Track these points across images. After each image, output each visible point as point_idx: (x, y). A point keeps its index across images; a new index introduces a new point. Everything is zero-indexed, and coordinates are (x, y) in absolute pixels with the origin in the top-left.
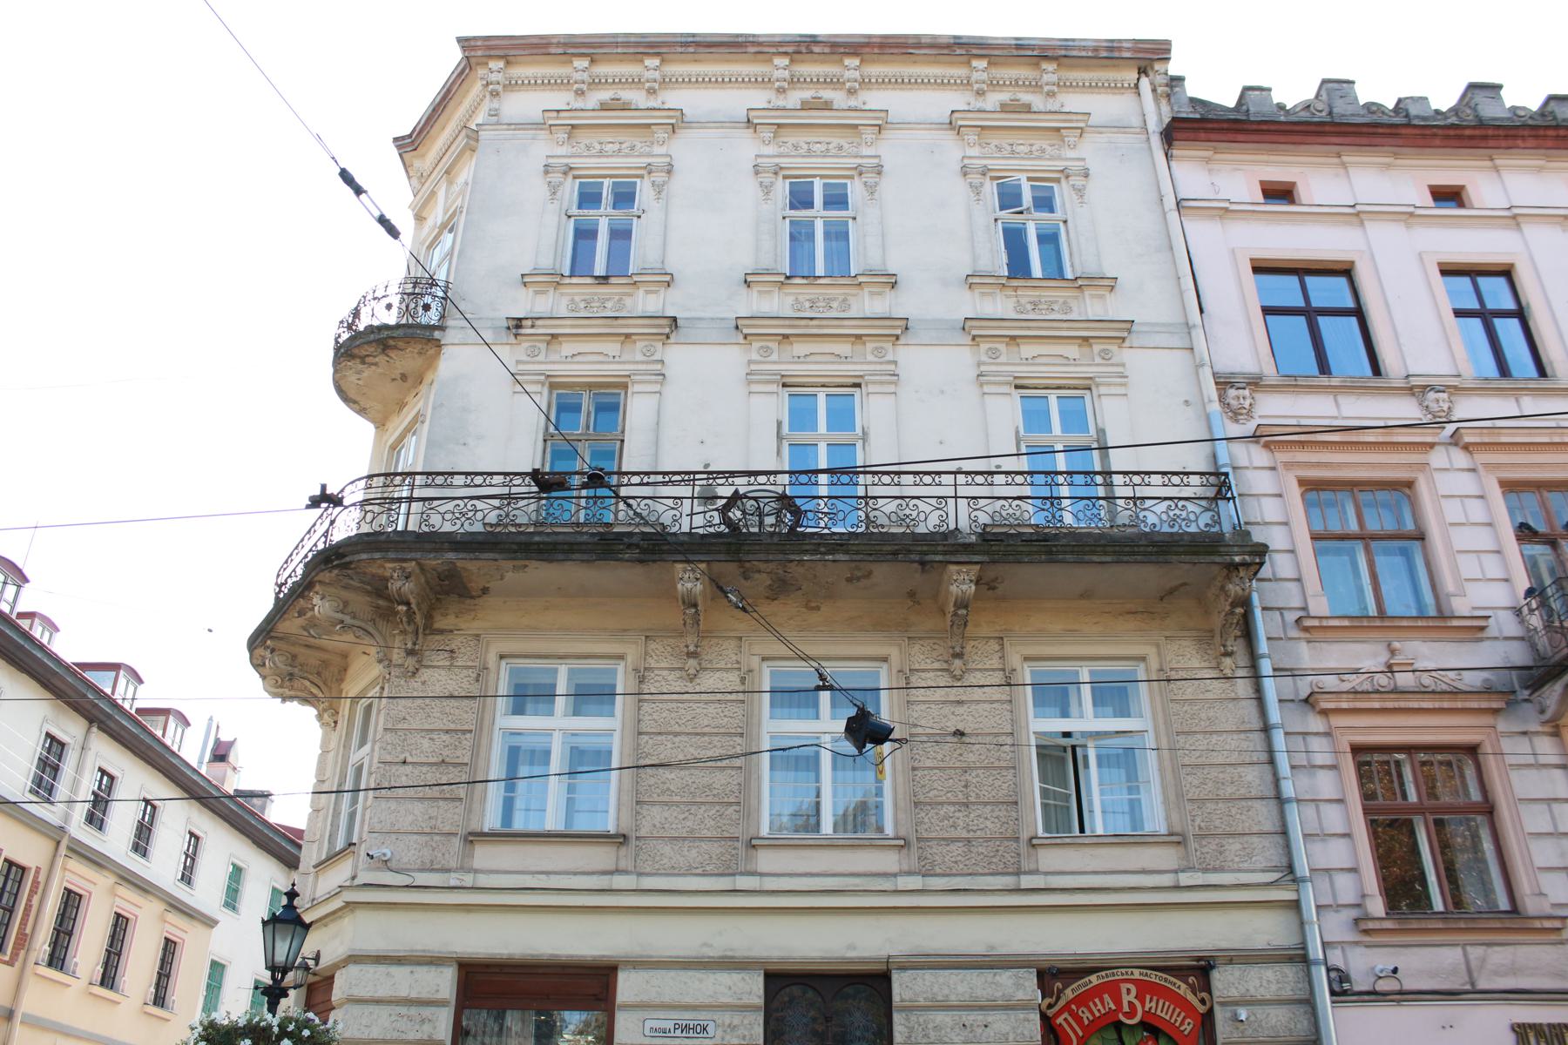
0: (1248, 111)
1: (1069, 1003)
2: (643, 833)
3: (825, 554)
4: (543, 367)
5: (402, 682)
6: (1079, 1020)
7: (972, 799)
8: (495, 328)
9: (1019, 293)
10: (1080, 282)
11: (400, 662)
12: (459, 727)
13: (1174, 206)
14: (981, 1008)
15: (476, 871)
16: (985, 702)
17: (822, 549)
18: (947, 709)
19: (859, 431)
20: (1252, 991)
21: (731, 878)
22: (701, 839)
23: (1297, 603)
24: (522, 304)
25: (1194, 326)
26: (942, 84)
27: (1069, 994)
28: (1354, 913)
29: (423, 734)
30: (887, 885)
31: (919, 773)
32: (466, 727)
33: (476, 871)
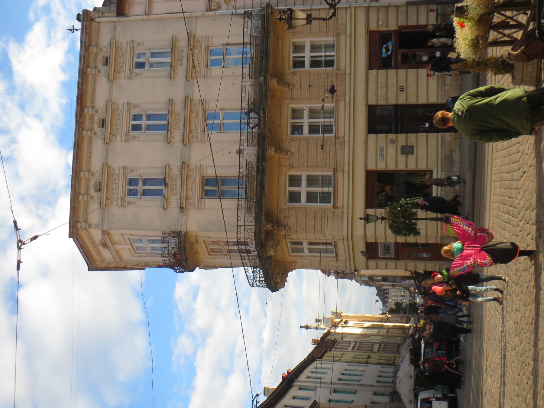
3: (266, 115)
5: (292, 230)
9: (176, 64)
13: (147, 16)
14: (377, 83)
15: (343, 204)
16: (301, 80)
17: (265, 115)
21: (345, 142)
25: (190, 15)
26: (94, 83)
31: (319, 97)
32: (305, 212)
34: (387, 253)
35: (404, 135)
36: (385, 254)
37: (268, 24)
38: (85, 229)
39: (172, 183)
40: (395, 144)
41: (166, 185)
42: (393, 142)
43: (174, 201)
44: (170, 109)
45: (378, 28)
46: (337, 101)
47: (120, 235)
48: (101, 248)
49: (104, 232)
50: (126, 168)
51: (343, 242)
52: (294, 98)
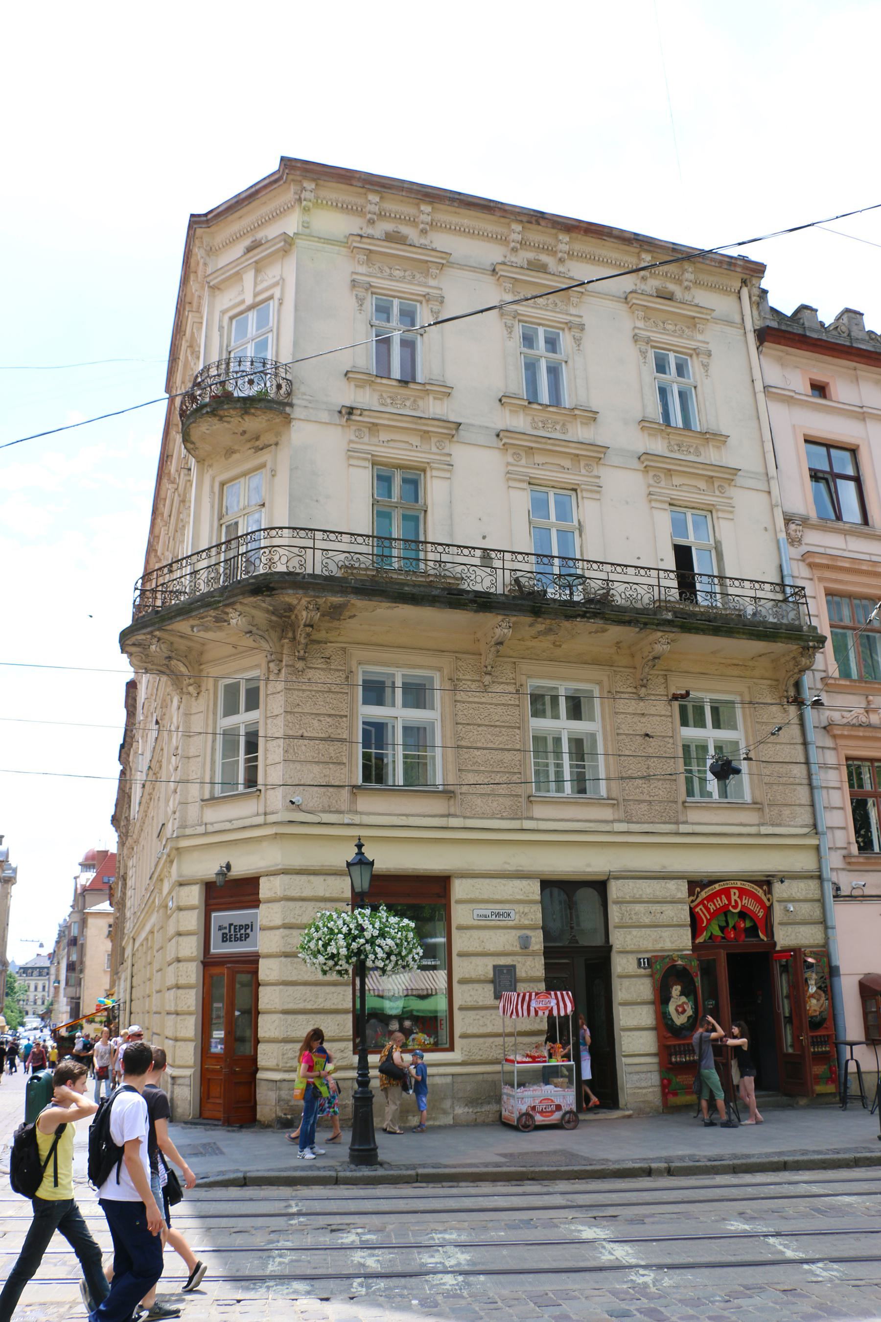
0: (803, 324)
1: (703, 900)
6: (708, 910)
8: (329, 410)
10: (708, 436)
11: (290, 663)
12: (337, 713)
13: (762, 389)
14: (658, 902)
15: (361, 813)
18: (636, 719)
19: (576, 523)
20: (794, 895)
22: (499, 795)
23: (822, 667)
24: (348, 396)
25: (773, 478)
28: (844, 852)
29: (313, 716)
32: (342, 713)
33: (361, 813)
34: (223, 934)
36: (221, 928)
37: (786, 638)
38: (300, 200)
39: (408, 399)
41: (404, 382)
42: (525, 943)
43: (364, 398)
44: (577, 412)
45: (778, 901)
46: (615, 802)
48: (247, 242)
50: (442, 302)
51: (258, 815)
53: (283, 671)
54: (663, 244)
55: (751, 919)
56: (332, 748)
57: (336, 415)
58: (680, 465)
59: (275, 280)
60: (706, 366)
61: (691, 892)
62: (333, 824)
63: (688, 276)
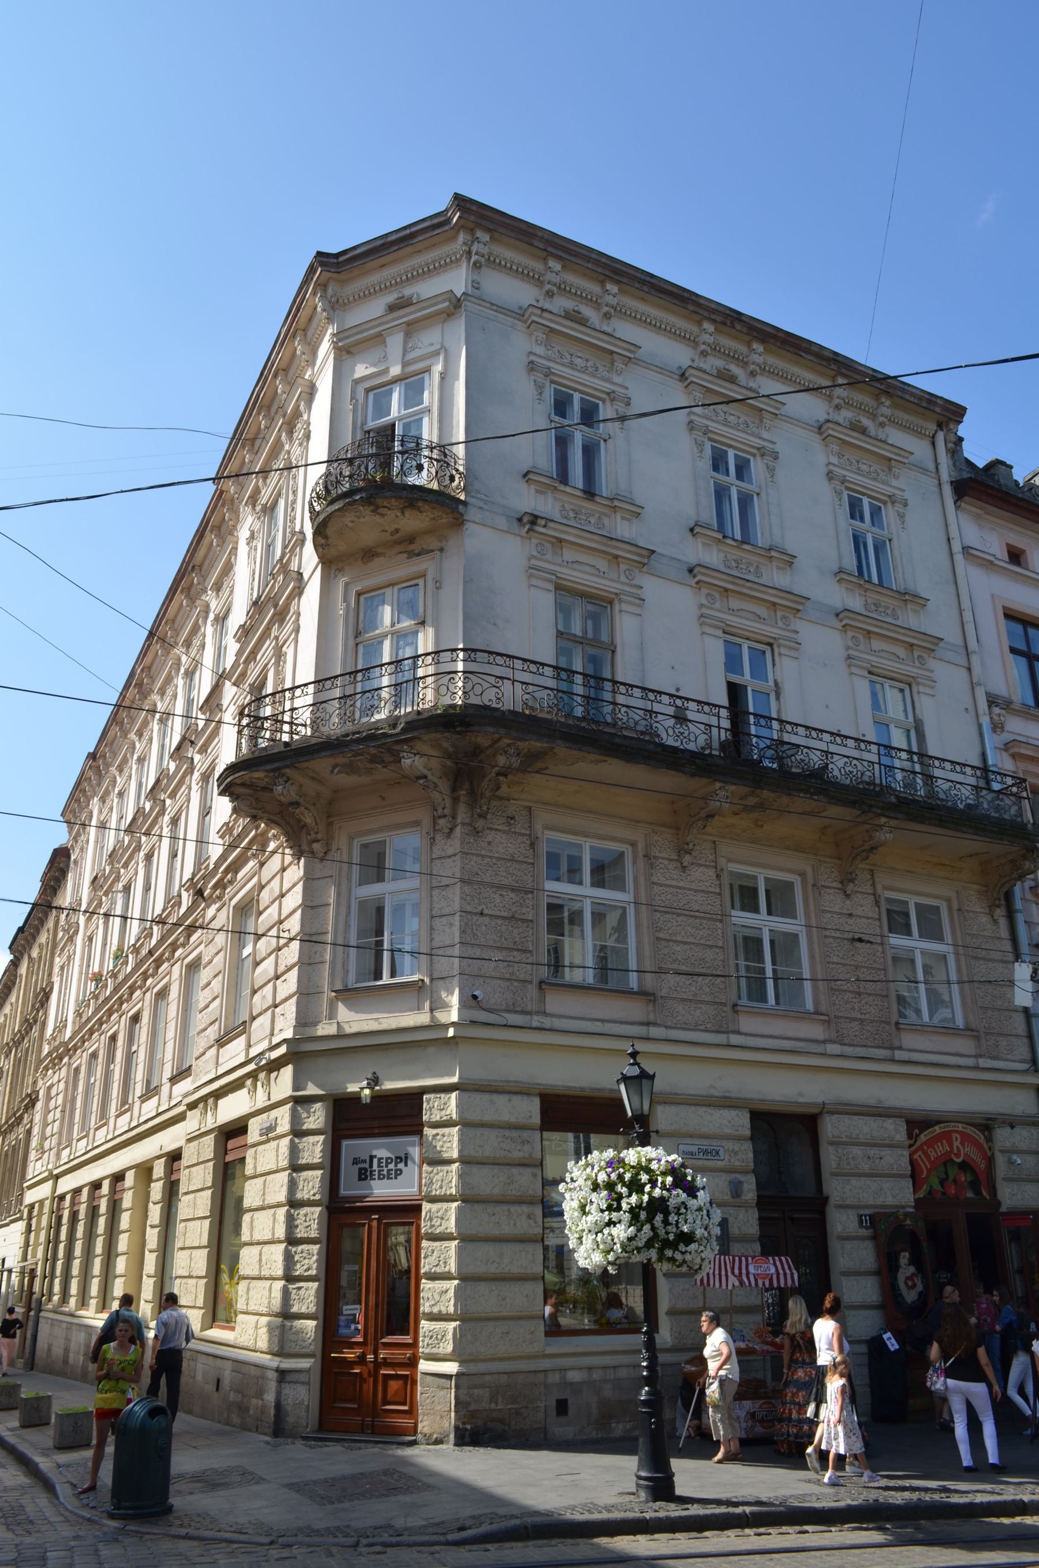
2: (663, 994)
4: (557, 568)
5: (472, 840)
6: (928, 1157)
7: (862, 990)
8: (508, 516)
10: (907, 597)
14: (875, 1145)
15: (552, 1015)
19: (771, 683)
24: (527, 500)
25: (975, 652)
27: (923, 1138)
29: (494, 890)
30: (819, 1049)
33: (552, 1015)
34: (360, 1169)
35: (754, 1230)
39: (593, 515)
40: (728, 1197)
42: (736, 1190)
43: (547, 505)
44: (773, 553)
46: (826, 1018)
47: (442, 344)
48: (391, 298)
49: (455, 304)
52: (822, 892)
53: (458, 829)
54: (863, 369)
55: (973, 1172)
56: (515, 931)
57: (515, 523)
58: (881, 628)
59: (432, 349)
60: (902, 516)
61: (910, 1136)
62: (522, 1027)
63: (884, 410)
